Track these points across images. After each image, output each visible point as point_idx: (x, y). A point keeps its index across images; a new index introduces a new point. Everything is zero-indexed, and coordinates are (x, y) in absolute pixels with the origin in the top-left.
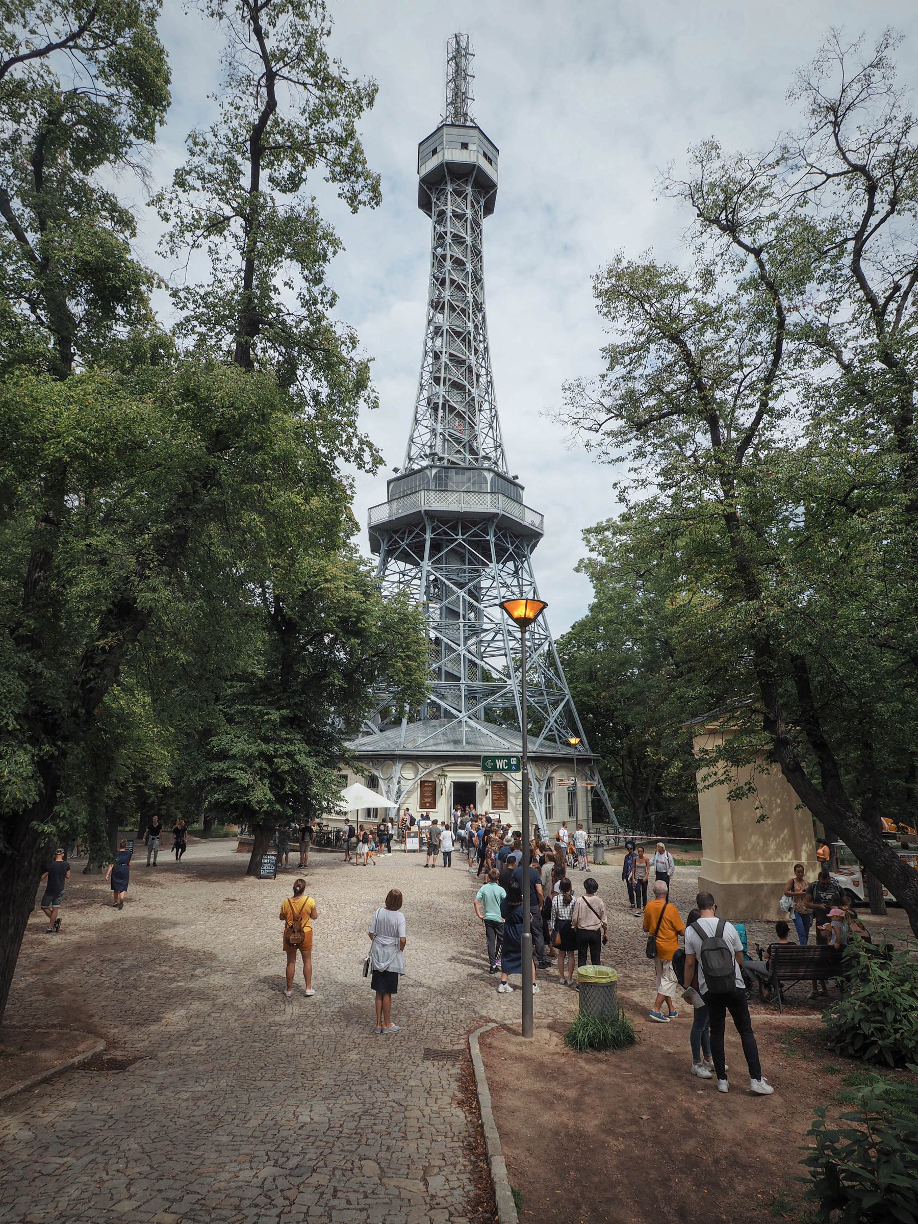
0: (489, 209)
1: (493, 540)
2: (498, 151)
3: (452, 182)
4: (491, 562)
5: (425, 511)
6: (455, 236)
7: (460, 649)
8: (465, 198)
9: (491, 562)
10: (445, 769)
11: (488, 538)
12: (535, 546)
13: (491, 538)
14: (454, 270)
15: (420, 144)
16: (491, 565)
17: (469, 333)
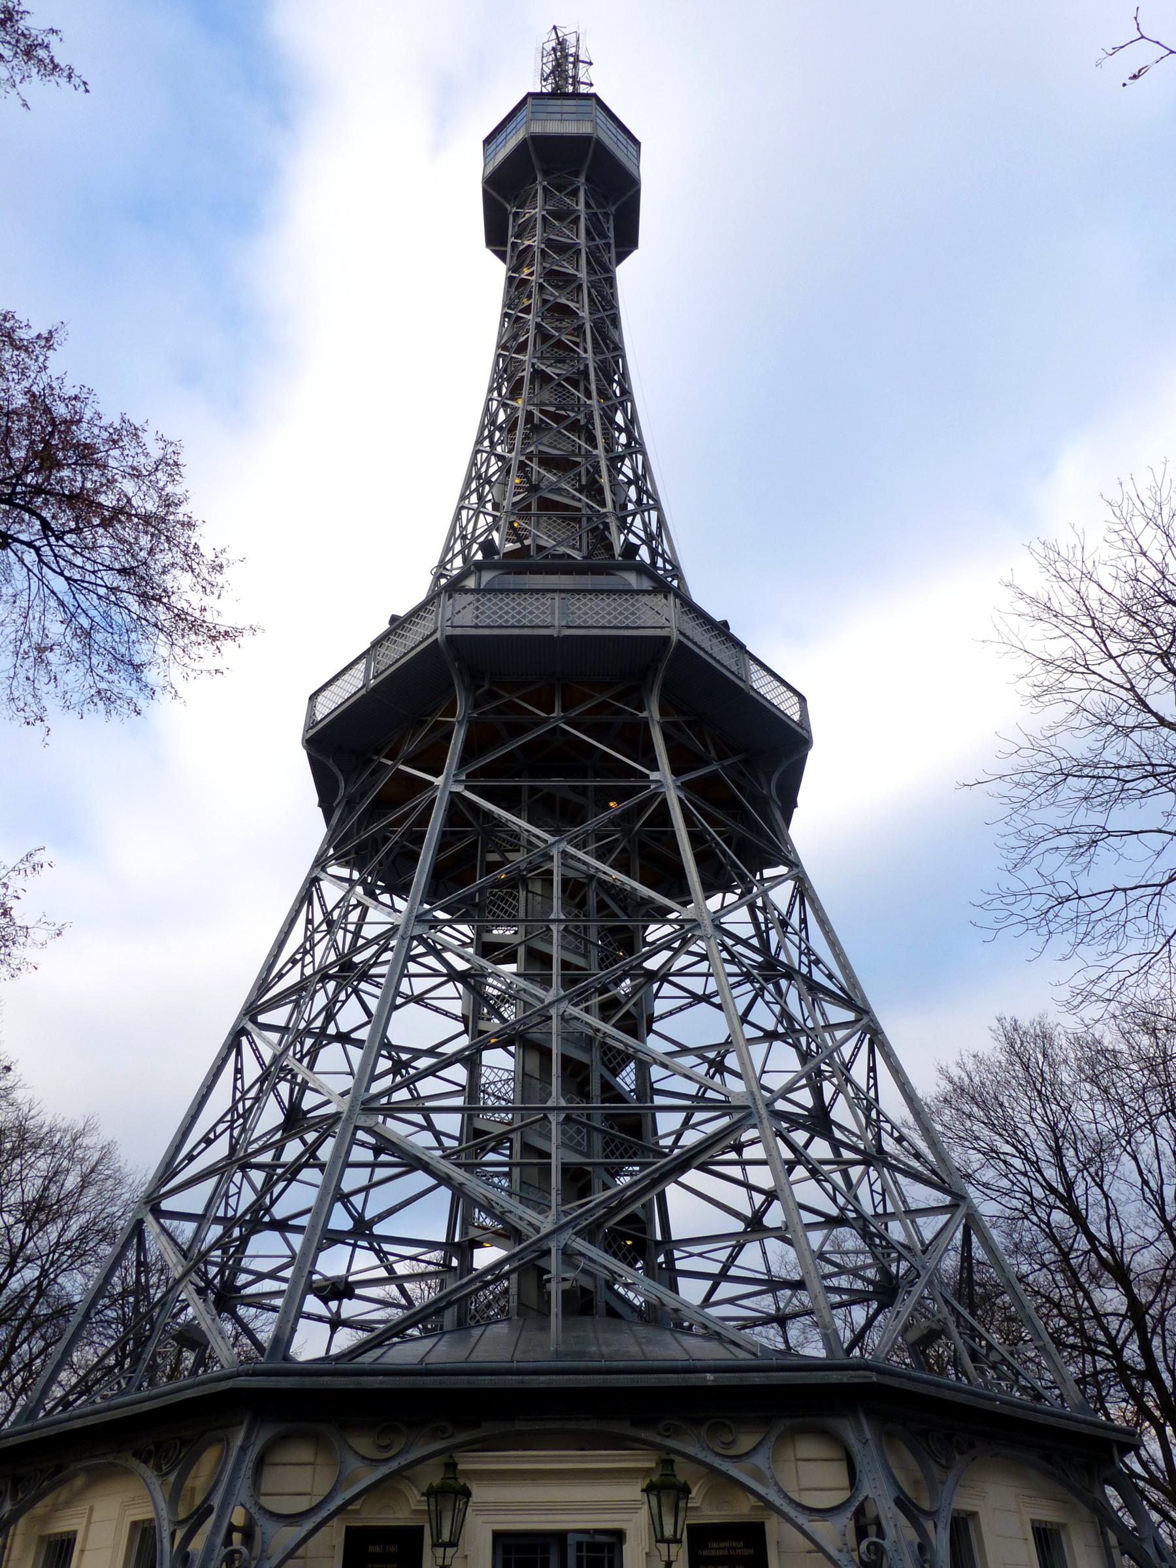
0: (627, 241)
1: (656, 716)
2: (637, 143)
3: (546, 173)
4: (655, 767)
5: (450, 639)
6: (550, 243)
7: (549, 997)
8: (574, 193)
9: (655, 767)
10: (468, 1463)
11: (645, 714)
12: (789, 804)
13: (653, 713)
14: (549, 285)
15: (488, 141)
16: (654, 776)
17: (585, 373)
